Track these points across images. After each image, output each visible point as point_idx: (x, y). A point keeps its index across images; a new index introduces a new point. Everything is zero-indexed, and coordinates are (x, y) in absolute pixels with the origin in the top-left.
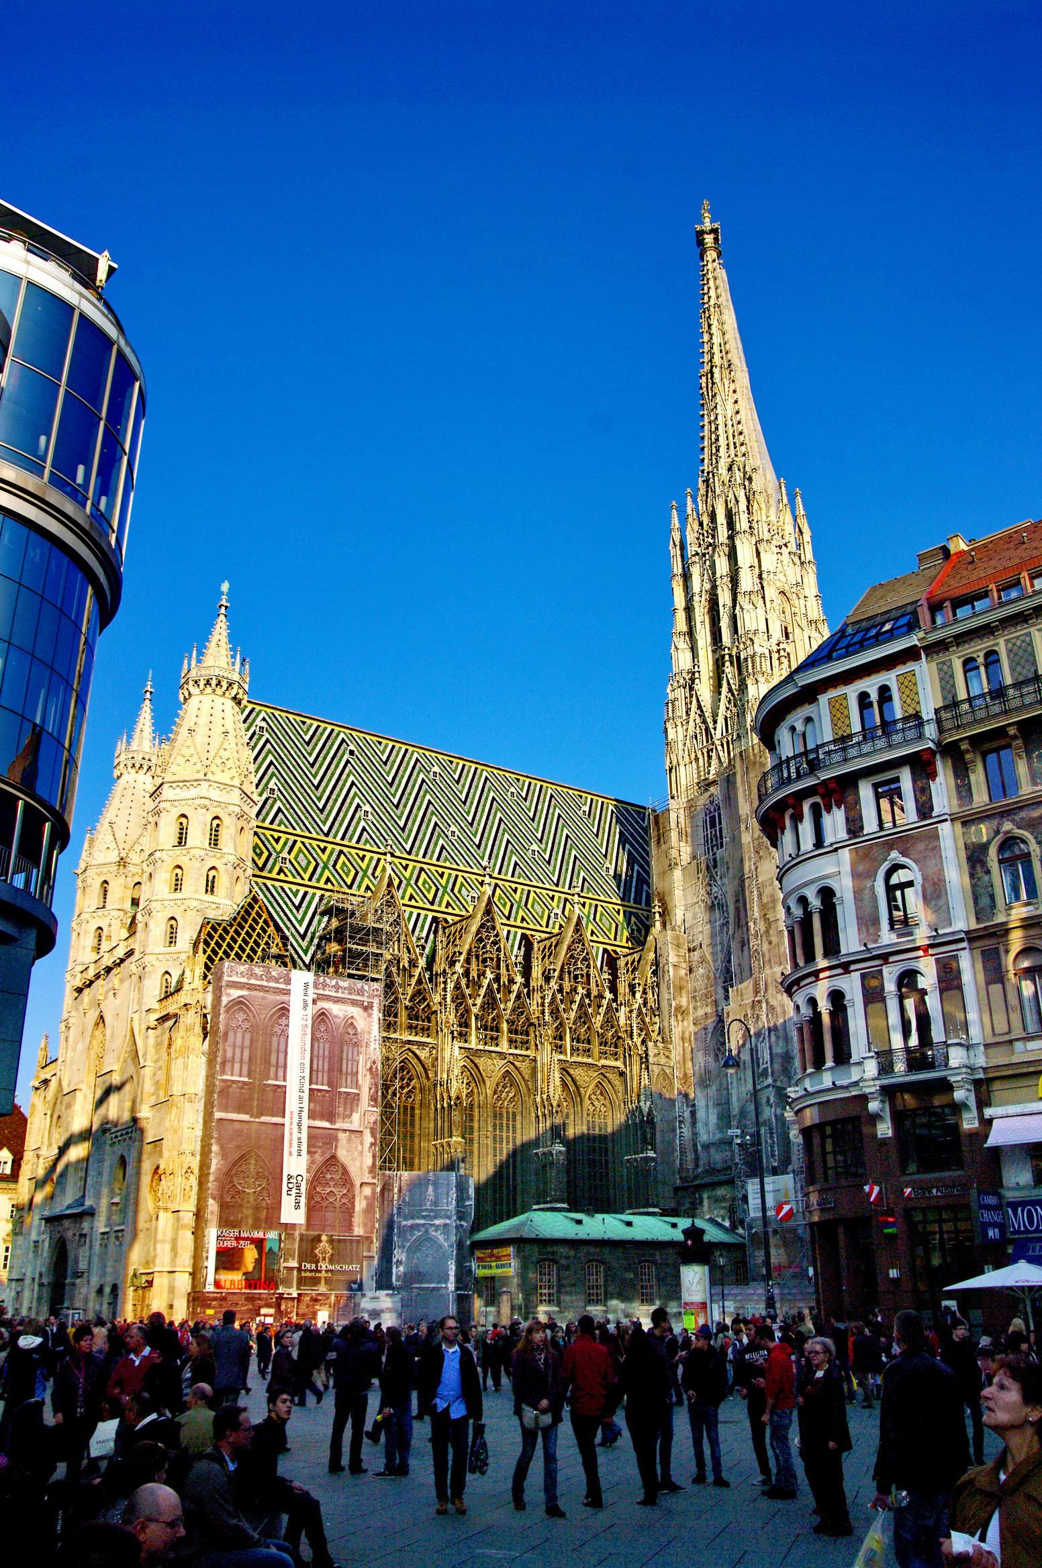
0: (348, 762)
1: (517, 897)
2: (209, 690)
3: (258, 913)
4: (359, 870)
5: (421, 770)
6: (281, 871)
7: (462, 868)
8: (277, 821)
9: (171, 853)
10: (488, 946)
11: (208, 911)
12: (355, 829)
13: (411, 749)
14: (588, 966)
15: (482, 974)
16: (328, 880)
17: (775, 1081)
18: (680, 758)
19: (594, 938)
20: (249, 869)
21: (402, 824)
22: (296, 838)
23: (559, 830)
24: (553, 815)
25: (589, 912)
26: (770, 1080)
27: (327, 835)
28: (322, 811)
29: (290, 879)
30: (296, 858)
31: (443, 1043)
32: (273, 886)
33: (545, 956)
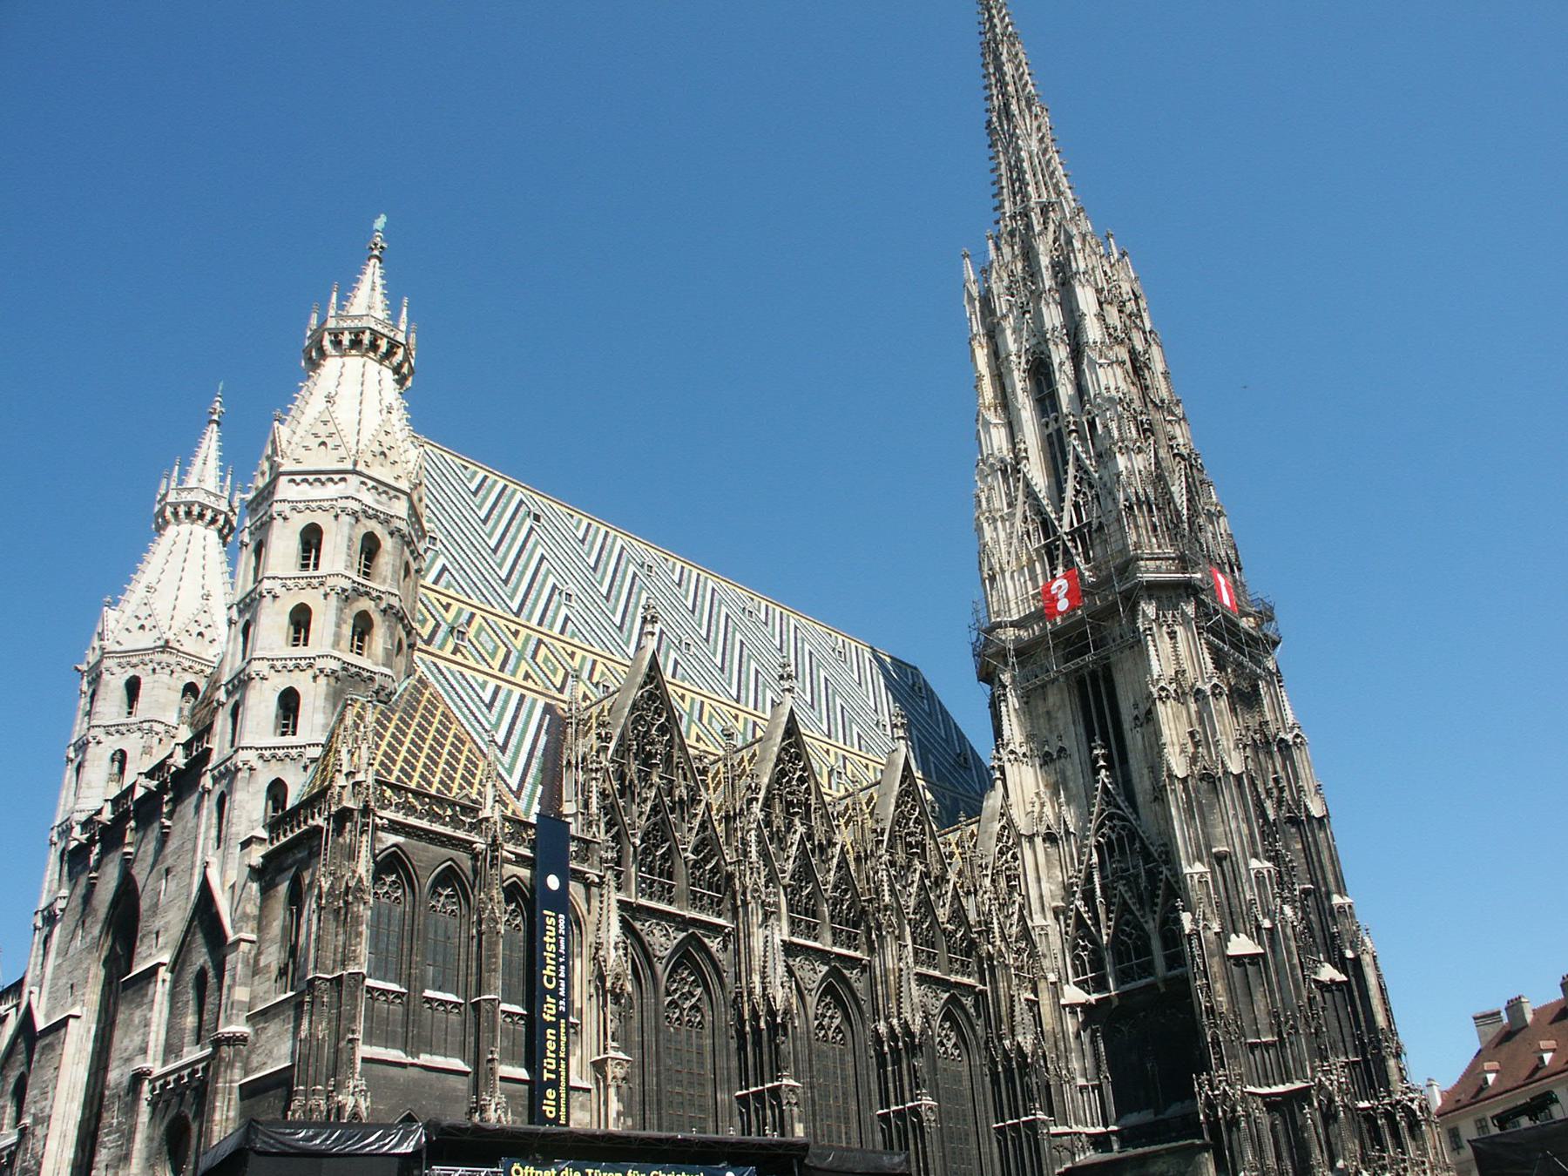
0: (532, 529)
5: (628, 562)
6: (456, 651)
7: (705, 692)
8: (443, 581)
10: (794, 783)
14: (923, 832)
15: (790, 827)
16: (527, 676)
18: (1004, 561)
21: (618, 621)
23: (815, 671)
27: (517, 614)
28: (506, 582)
29: (472, 663)
30: (477, 636)
31: (748, 925)
32: (448, 669)
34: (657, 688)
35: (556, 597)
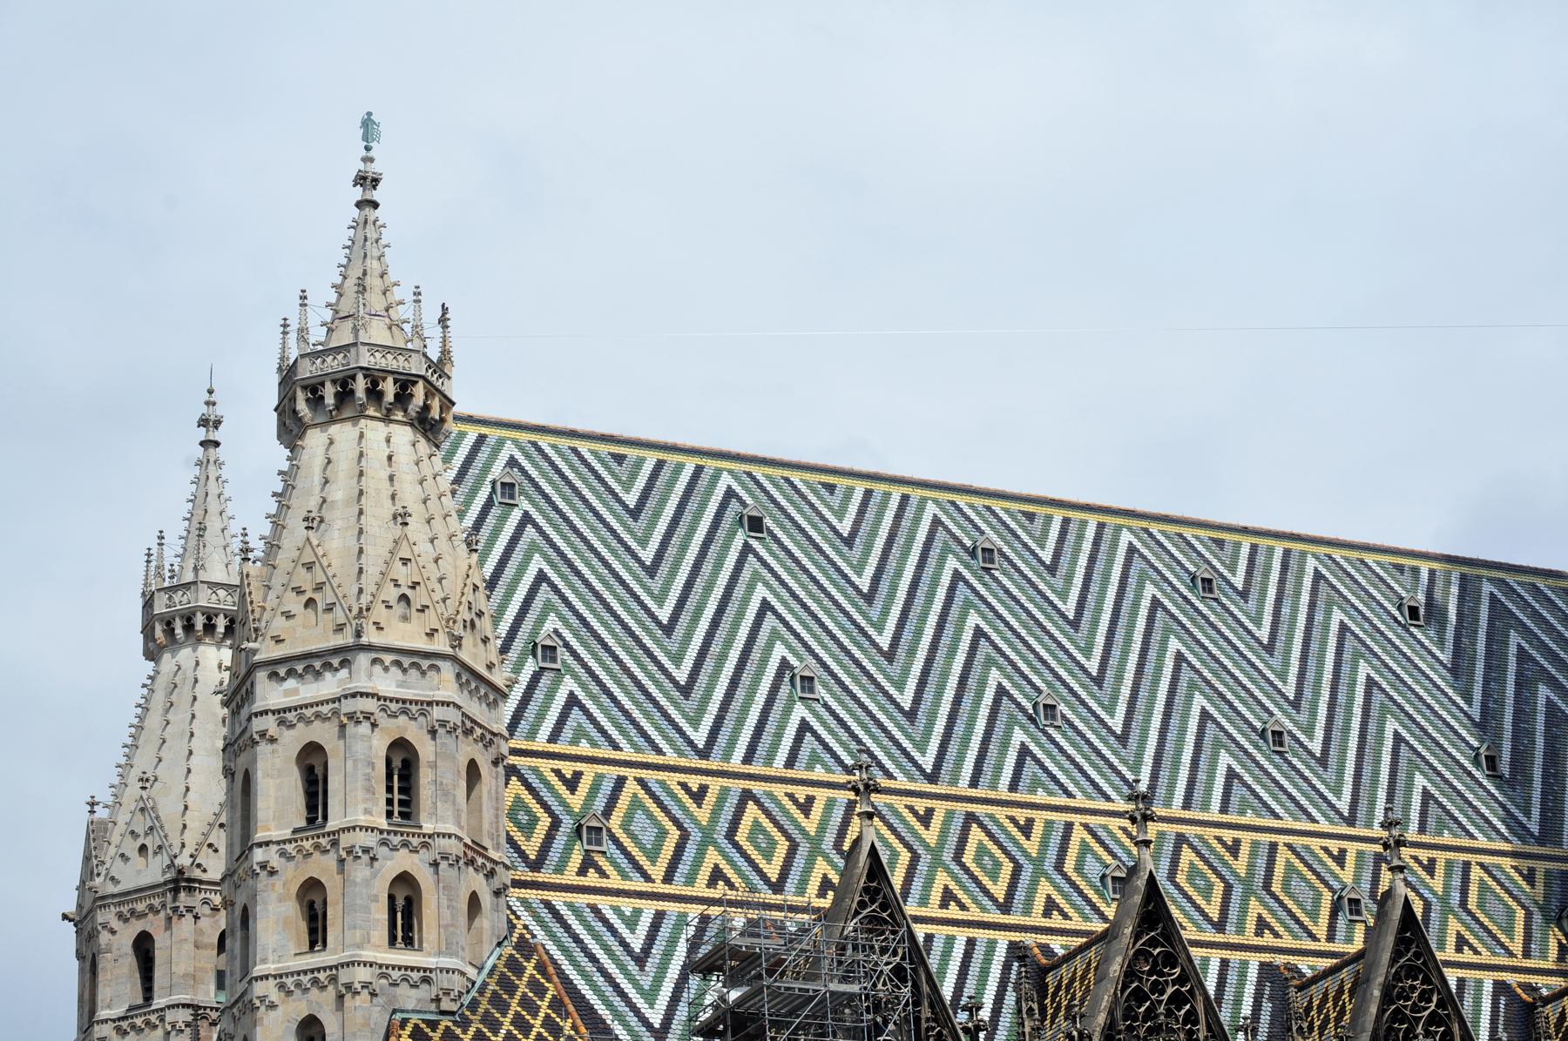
0: (747, 549)
1: (1241, 866)
2: (347, 413)
4: (798, 837)
5: (946, 550)
6: (587, 864)
7: (1080, 801)
8: (567, 733)
9: (289, 848)
11: (398, 990)
12: (781, 728)
16: (716, 876)
19: (1467, 956)
20: (500, 869)
21: (906, 701)
22: (623, 771)
23: (1346, 669)
24: (1326, 627)
25: (1447, 887)
27: (704, 754)
28: (686, 690)
29: (615, 882)
32: (570, 906)
33: (1326, 1021)
34: (884, 907)
35: (785, 689)
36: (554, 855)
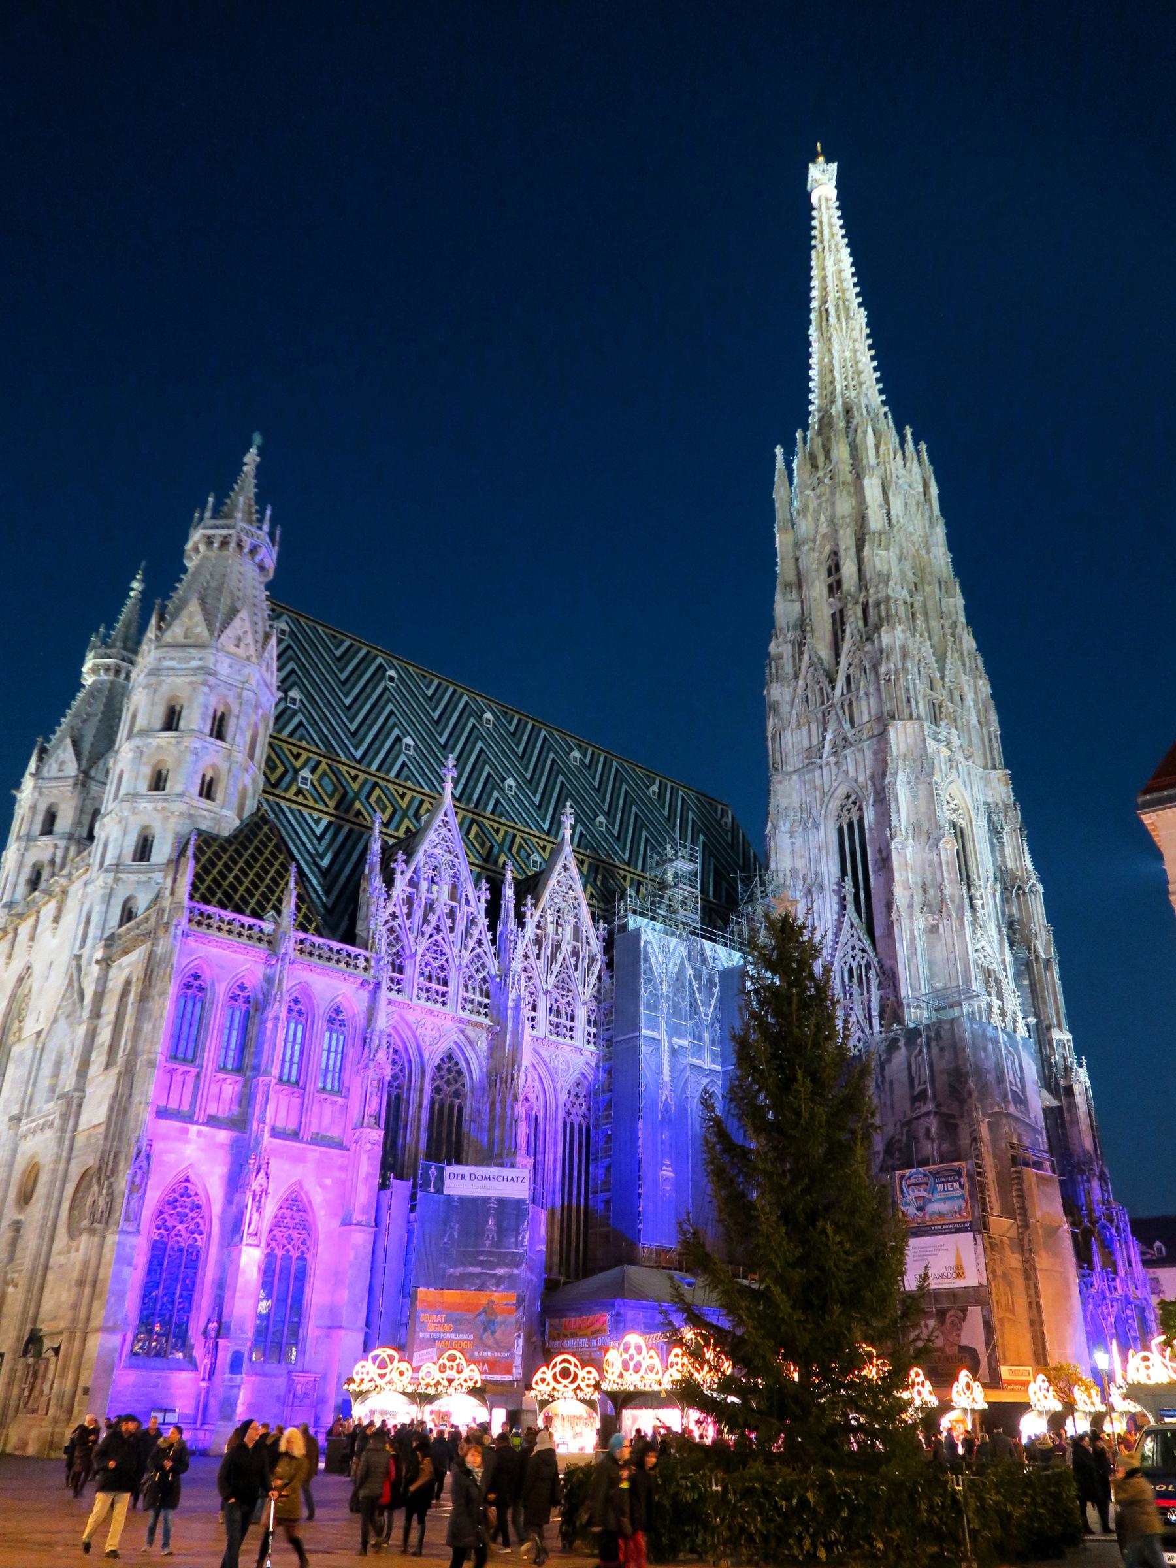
0: (386, 689)
3: (266, 835)
6: (299, 792)
7: (520, 826)
8: (297, 735)
13: (460, 690)
15: (557, 947)
17: (938, 1106)
24: (620, 789)
26: (930, 1106)
27: (359, 762)
29: (311, 803)
30: (319, 781)
32: (288, 807)
35: (397, 747)
36: (284, 784)
